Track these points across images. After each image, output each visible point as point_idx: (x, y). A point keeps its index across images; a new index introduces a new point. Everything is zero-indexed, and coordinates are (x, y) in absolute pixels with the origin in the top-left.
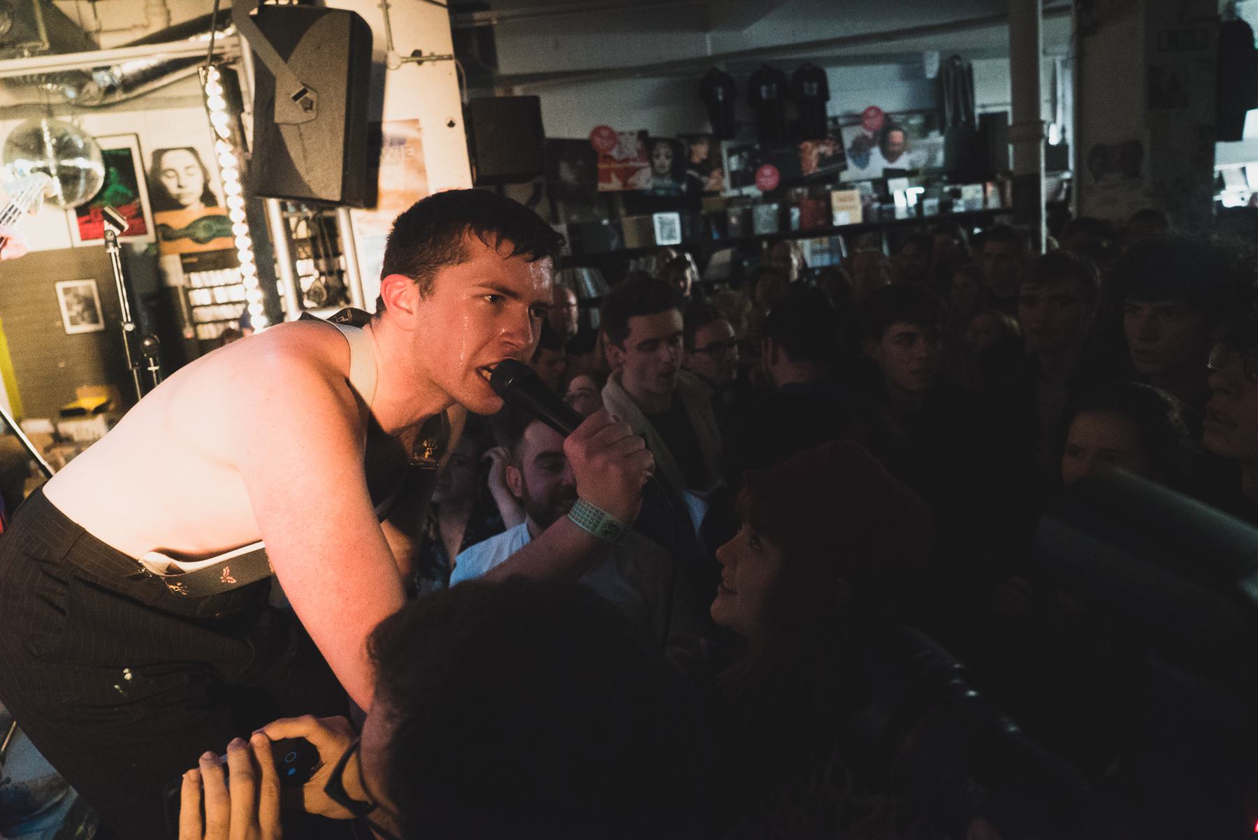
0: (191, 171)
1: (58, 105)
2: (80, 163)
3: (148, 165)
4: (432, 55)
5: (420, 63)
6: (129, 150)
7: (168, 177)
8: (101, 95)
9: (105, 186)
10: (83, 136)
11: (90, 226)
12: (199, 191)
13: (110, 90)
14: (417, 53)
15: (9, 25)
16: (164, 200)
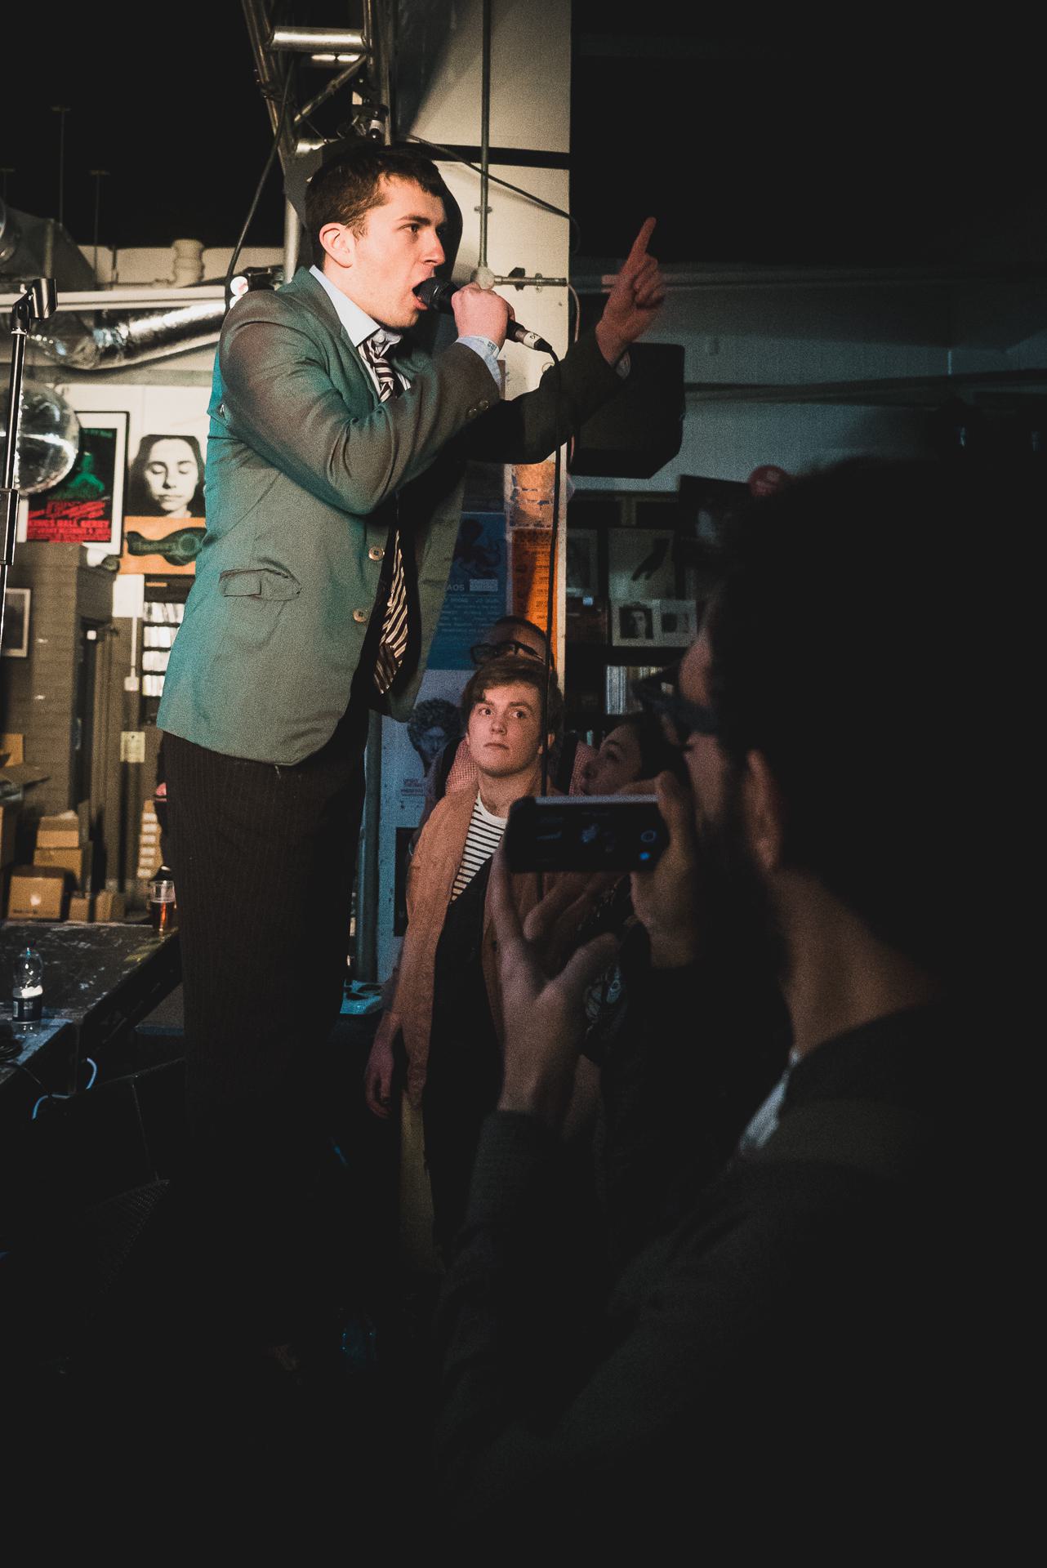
0: (184, 468)
1: (43, 367)
2: (51, 439)
3: (133, 454)
4: (538, 276)
5: (519, 286)
6: (114, 431)
7: (155, 473)
8: (97, 357)
9: (74, 473)
10: (63, 406)
11: (40, 523)
12: (189, 493)
13: (110, 352)
14: (518, 273)
15: (12, 250)
16: (142, 501)
